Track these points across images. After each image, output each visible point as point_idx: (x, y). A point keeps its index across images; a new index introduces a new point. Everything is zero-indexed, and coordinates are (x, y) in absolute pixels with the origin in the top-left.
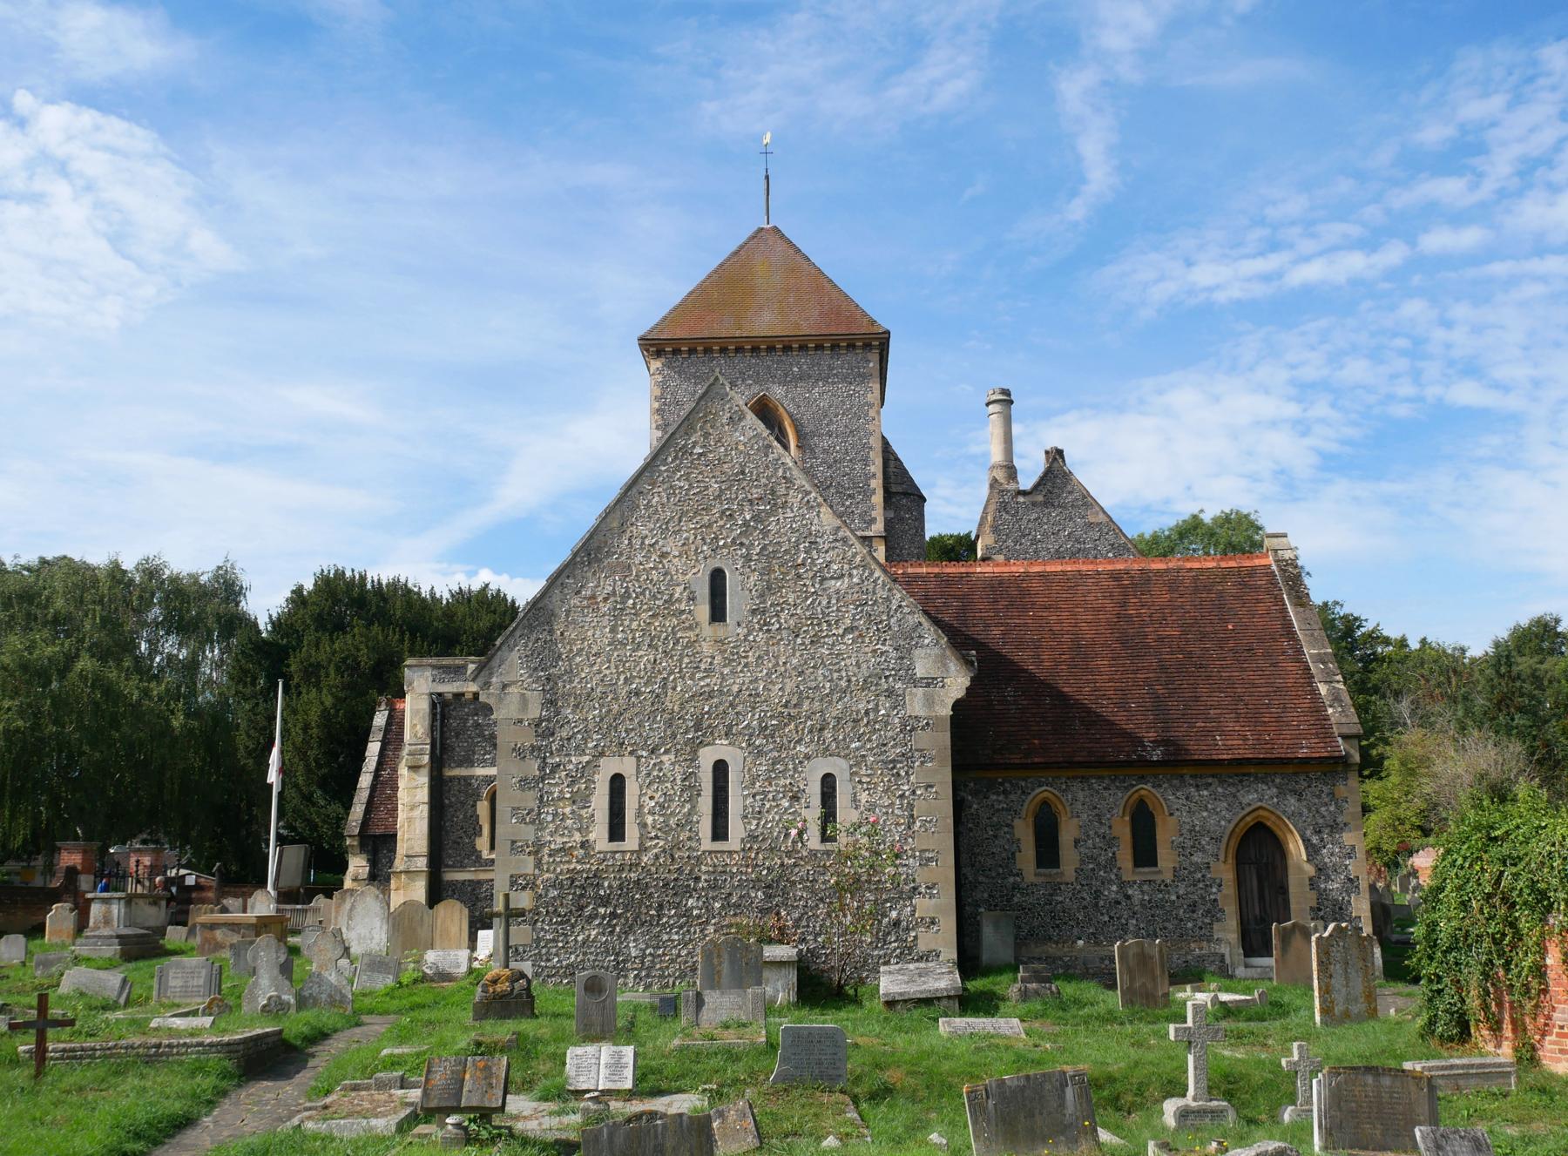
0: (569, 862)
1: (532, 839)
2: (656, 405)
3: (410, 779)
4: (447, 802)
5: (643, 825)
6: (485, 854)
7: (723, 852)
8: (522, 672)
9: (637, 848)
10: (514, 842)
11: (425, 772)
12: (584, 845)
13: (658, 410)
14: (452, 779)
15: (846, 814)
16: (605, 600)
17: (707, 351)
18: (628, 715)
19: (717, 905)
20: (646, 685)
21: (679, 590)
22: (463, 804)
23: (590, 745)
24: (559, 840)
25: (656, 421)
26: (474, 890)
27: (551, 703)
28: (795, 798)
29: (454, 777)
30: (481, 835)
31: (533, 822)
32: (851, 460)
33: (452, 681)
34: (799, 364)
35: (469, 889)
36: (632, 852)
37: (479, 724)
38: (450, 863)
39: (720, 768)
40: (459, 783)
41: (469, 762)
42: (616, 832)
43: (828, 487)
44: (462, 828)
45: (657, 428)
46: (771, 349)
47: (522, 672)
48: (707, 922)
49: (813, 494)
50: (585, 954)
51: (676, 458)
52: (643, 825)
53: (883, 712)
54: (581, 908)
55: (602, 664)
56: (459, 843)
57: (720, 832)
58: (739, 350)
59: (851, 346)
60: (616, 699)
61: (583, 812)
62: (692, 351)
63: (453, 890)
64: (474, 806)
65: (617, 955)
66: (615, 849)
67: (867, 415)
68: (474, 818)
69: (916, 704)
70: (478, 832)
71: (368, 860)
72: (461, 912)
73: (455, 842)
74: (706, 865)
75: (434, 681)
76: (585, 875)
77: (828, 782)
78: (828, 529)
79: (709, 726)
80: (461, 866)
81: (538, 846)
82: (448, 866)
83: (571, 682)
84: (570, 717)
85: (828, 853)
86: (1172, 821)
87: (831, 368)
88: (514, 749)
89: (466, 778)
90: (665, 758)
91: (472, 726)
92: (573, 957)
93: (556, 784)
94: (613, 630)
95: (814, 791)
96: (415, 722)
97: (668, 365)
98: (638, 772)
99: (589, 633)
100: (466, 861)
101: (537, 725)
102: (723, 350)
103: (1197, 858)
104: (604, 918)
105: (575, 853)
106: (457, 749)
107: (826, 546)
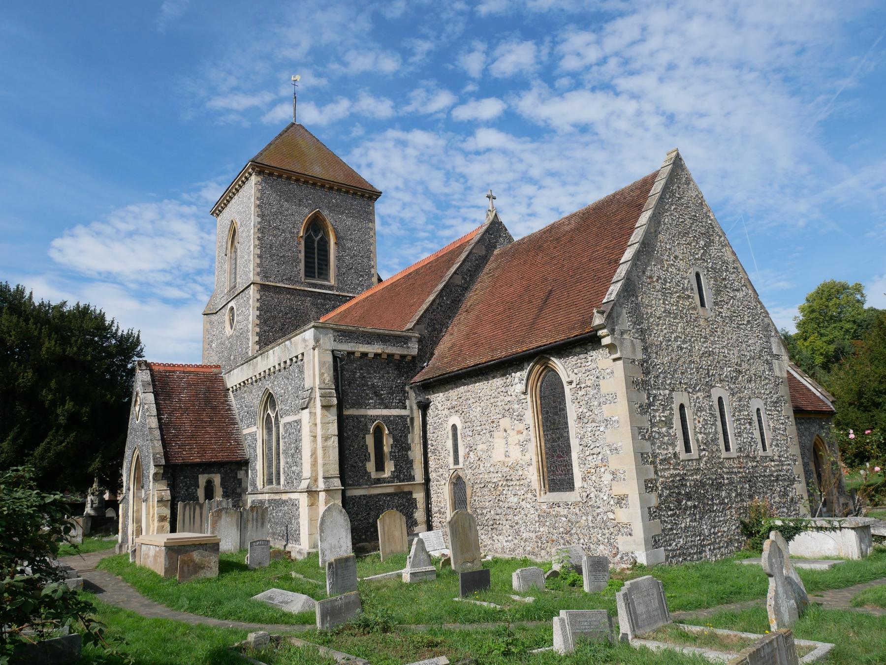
0: (669, 469)
1: (650, 451)
2: (258, 202)
3: (323, 416)
4: (345, 434)
5: (697, 440)
6: (374, 475)
7: (730, 458)
8: (629, 324)
9: (698, 457)
10: (642, 454)
11: (334, 410)
12: (675, 454)
13: (258, 206)
14: (348, 417)
16: (657, 280)
17: (289, 178)
18: (680, 363)
19: (734, 495)
20: (684, 342)
21: (686, 281)
22: (357, 436)
23: (668, 382)
25: (257, 212)
26: (367, 502)
27: (645, 349)
28: (750, 423)
29: (349, 415)
30: (369, 461)
31: (649, 439)
32: (362, 256)
33: (346, 342)
34: (336, 199)
36: (696, 460)
37: (364, 377)
38: (350, 482)
40: (353, 421)
41: (366, 406)
42: (688, 449)
43: (351, 269)
44: (357, 456)
45: (258, 216)
46: (323, 186)
47: (629, 324)
48: (731, 507)
49: (722, 238)
50: (687, 537)
51: (670, 197)
52: (697, 440)
53: (767, 373)
54: (679, 502)
55: (663, 325)
56: (355, 467)
58: (306, 182)
59: (363, 196)
60: (672, 350)
61: (671, 431)
62: (280, 176)
63: (353, 504)
64: (364, 438)
65: (700, 536)
66: (689, 458)
67: (369, 234)
68: (364, 448)
71: (168, 485)
72: (401, 520)
73: (352, 466)
74: (726, 468)
75: (335, 341)
76: (678, 478)
78: (731, 260)
79: (712, 375)
80: (358, 485)
81: (655, 456)
82: (351, 485)
83: (651, 335)
84: (656, 360)
88: (633, 382)
89: (357, 417)
90: (699, 394)
91: (360, 377)
92: (681, 540)
93: (657, 410)
94: (664, 303)
96: (323, 371)
97: (264, 181)
98: (690, 403)
99: (653, 302)
100: (361, 481)
101: (642, 365)
102: (297, 180)
104: (691, 507)
105: (672, 462)
106: (350, 395)
107: (732, 270)
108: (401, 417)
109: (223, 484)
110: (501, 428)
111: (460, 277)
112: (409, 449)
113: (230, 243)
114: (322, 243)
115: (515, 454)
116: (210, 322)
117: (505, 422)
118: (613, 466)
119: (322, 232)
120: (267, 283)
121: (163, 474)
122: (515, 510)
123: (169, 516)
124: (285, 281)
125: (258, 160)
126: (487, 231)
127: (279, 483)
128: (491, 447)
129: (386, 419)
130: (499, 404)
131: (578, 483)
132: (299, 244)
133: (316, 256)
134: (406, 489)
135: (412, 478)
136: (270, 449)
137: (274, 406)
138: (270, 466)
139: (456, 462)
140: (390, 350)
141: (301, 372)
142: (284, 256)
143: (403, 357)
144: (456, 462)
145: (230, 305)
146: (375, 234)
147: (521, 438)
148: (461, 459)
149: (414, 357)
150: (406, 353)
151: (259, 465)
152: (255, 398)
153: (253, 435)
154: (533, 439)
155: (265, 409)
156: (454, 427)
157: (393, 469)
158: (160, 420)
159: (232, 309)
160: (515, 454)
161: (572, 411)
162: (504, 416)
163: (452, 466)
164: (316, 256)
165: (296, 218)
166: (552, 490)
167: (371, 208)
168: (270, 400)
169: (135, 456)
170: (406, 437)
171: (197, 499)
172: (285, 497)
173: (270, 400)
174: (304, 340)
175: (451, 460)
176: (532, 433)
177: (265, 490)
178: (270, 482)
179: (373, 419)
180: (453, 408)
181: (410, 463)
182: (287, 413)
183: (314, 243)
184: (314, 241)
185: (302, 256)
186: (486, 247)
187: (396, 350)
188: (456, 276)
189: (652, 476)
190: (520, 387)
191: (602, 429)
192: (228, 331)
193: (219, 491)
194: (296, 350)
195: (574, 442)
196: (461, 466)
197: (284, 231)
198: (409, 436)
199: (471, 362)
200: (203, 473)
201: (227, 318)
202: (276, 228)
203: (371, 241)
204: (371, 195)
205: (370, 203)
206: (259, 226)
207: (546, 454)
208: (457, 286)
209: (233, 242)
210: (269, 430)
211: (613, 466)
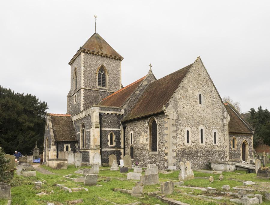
6: (110, 146)
11: (99, 128)
14: (103, 130)
15: (217, 140)
24: (180, 142)
35: (107, 152)
39: (202, 130)
57: (202, 142)
64: (107, 136)
77: (215, 133)
85: (215, 145)
86: (237, 141)
95: (213, 135)
102: (96, 55)
108: (118, 131)
110: (142, 135)
111: (138, 91)
112: (120, 139)
113: (75, 75)
114: (104, 75)
115: (145, 141)
116: (69, 99)
117: (143, 133)
118: (165, 145)
119: (104, 72)
120: (86, 88)
121: (54, 144)
122: (144, 156)
123: (56, 155)
126: (148, 77)
127: (85, 147)
128: (140, 139)
129: (114, 131)
130: (142, 128)
131: (158, 150)
132: (96, 76)
134: (119, 150)
135: (121, 147)
136: (83, 138)
137: (84, 127)
138: (83, 143)
139: (132, 143)
140: (116, 112)
141: (91, 118)
142: (91, 80)
143: (119, 114)
144: (132, 143)
145: (75, 94)
146: (121, 72)
147: (146, 137)
148: (133, 142)
149: (123, 114)
150: (120, 113)
151: (81, 142)
152: (80, 124)
153: (79, 134)
154: (149, 138)
155: (82, 127)
156: (132, 134)
157: (115, 144)
158: (53, 130)
159: (76, 96)
160: (145, 141)
161: (158, 131)
162: (143, 132)
163: (130, 144)
164: (102, 79)
165: (95, 67)
166: (152, 151)
168: (83, 125)
169: (47, 139)
171: (64, 151)
172: (87, 151)
173: (83, 125)
174: (91, 110)
175: (130, 142)
176: (149, 136)
177: (82, 149)
178: (83, 147)
179: (110, 131)
180: (132, 129)
181: (120, 143)
182: (87, 129)
183: (101, 76)
184: (101, 74)
185: (97, 80)
187: (118, 113)
188: (137, 91)
189: (175, 148)
190: (147, 124)
191: (164, 136)
192: (75, 102)
193: (70, 149)
194: (90, 112)
195: (158, 139)
196: (133, 144)
199: (136, 117)
200: (65, 144)
201: (74, 98)
202: (89, 71)
204: (120, 59)
205: (120, 62)
206: (83, 70)
207: (152, 142)
209: (76, 74)
210: (83, 133)
211: (165, 145)
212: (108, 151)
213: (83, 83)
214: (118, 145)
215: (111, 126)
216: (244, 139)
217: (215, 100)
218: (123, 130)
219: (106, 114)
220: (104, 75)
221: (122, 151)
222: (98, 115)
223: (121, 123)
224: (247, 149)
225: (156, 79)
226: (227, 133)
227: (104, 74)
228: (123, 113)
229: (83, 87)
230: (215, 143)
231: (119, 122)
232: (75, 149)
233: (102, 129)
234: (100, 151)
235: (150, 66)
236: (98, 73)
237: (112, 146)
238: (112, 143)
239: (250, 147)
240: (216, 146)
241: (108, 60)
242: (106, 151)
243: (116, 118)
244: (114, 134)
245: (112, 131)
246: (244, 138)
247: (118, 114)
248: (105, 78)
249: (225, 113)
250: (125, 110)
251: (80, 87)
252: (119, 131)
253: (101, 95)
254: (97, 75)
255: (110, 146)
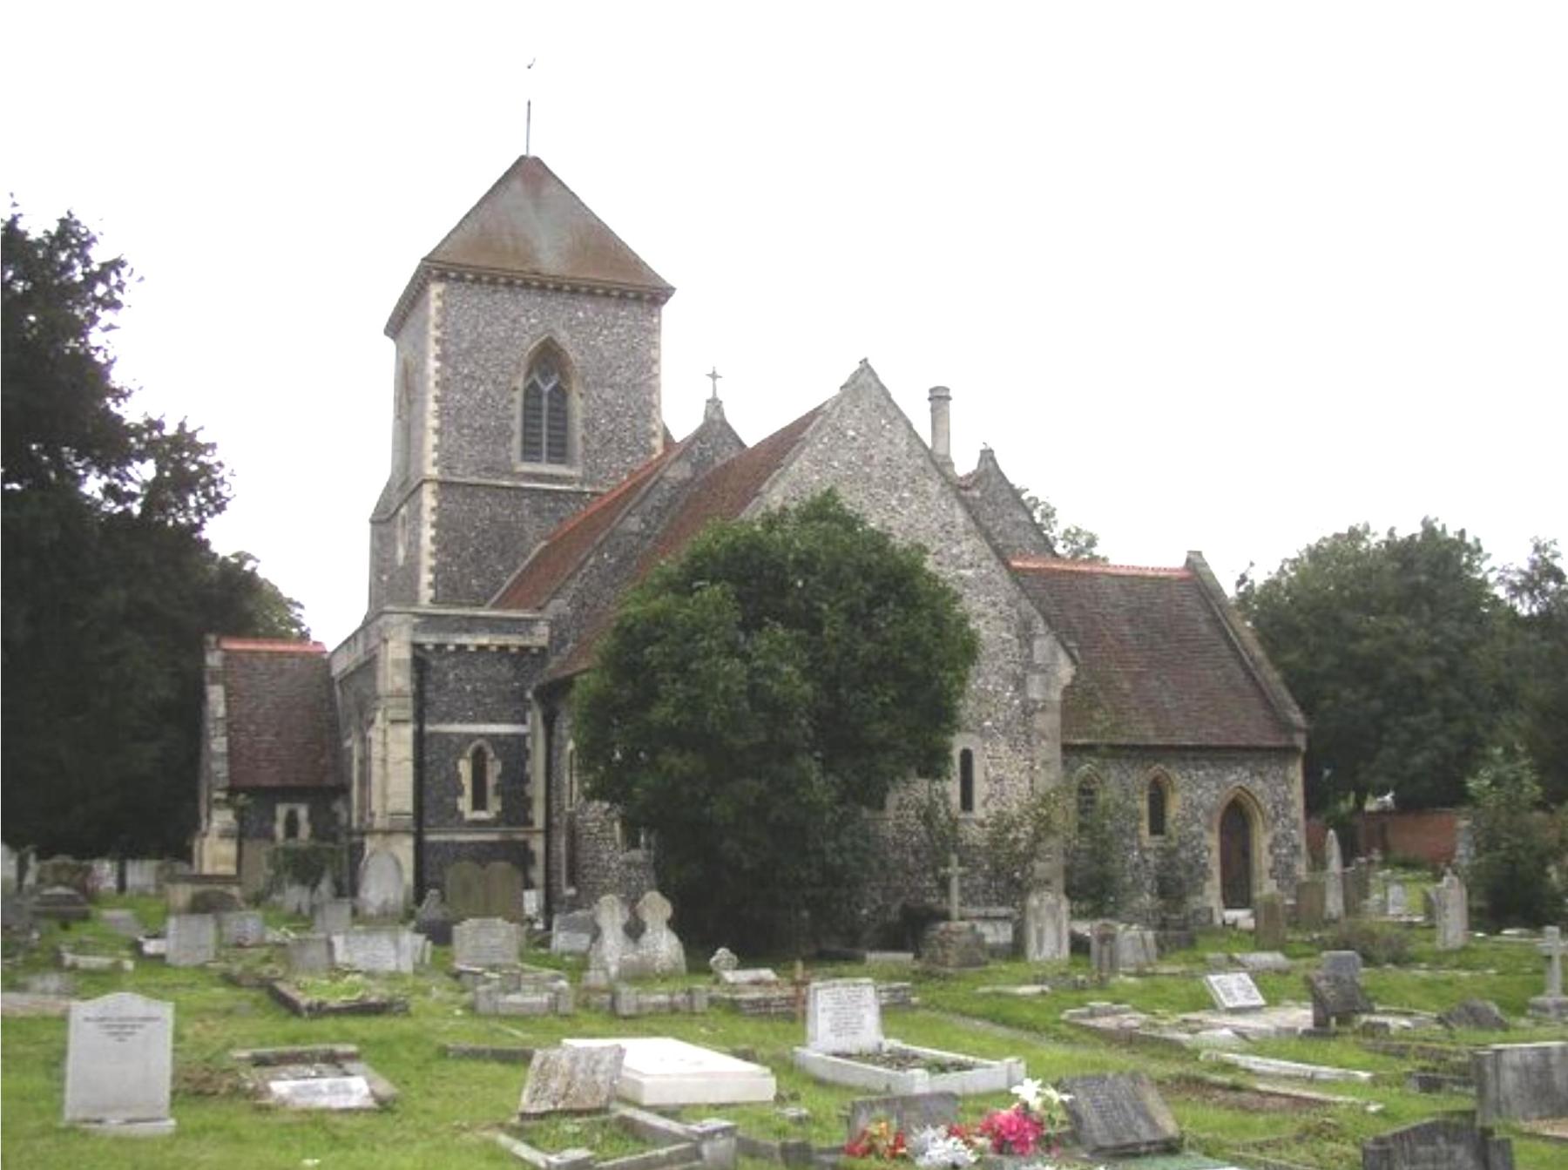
14: (433, 735)
15: (981, 788)
17: (493, 281)
46: (558, 289)
69: (1035, 692)
70: (460, 792)
80: (441, 826)
82: (429, 826)
87: (616, 317)
102: (510, 284)
103: (1195, 828)
108: (514, 735)
109: (311, 818)
114: (557, 396)
124: (483, 473)
125: (436, 258)
129: (493, 739)
133: (545, 421)
134: (520, 837)
135: (531, 823)
142: (480, 428)
143: (524, 650)
149: (542, 649)
150: (527, 642)
153: (350, 749)
167: (655, 320)
170: (523, 765)
179: (470, 737)
181: (528, 803)
185: (517, 425)
186: (693, 464)
187: (514, 641)
197: (482, 382)
198: (528, 764)
202: (471, 377)
203: (653, 382)
208: (632, 533)
212: (461, 844)
213: (436, 448)
214: (516, 810)
215: (475, 714)
216: (1237, 778)
217: (969, 573)
218: (541, 731)
219: (451, 648)
220: (560, 395)
221: (538, 845)
222: (405, 654)
223: (536, 694)
224: (1262, 840)
225: (741, 444)
226: (1049, 750)
227: (557, 388)
228: (544, 641)
229: (432, 472)
230: (967, 803)
231: (523, 689)
232: (333, 829)
233: (429, 728)
234: (409, 842)
235: (714, 376)
236: (520, 383)
237: (482, 815)
238: (479, 802)
239: (1279, 829)
240: (976, 827)
241: (584, 310)
242: (446, 843)
243: (505, 670)
244: (491, 755)
245: (481, 736)
246: (1233, 777)
247: (514, 650)
248: (565, 412)
249: (1037, 643)
250: (553, 624)
251: (420, 471)
252: (521, 738)
253: (538, 512)
254: (518, 396)
255: (470, 815)
